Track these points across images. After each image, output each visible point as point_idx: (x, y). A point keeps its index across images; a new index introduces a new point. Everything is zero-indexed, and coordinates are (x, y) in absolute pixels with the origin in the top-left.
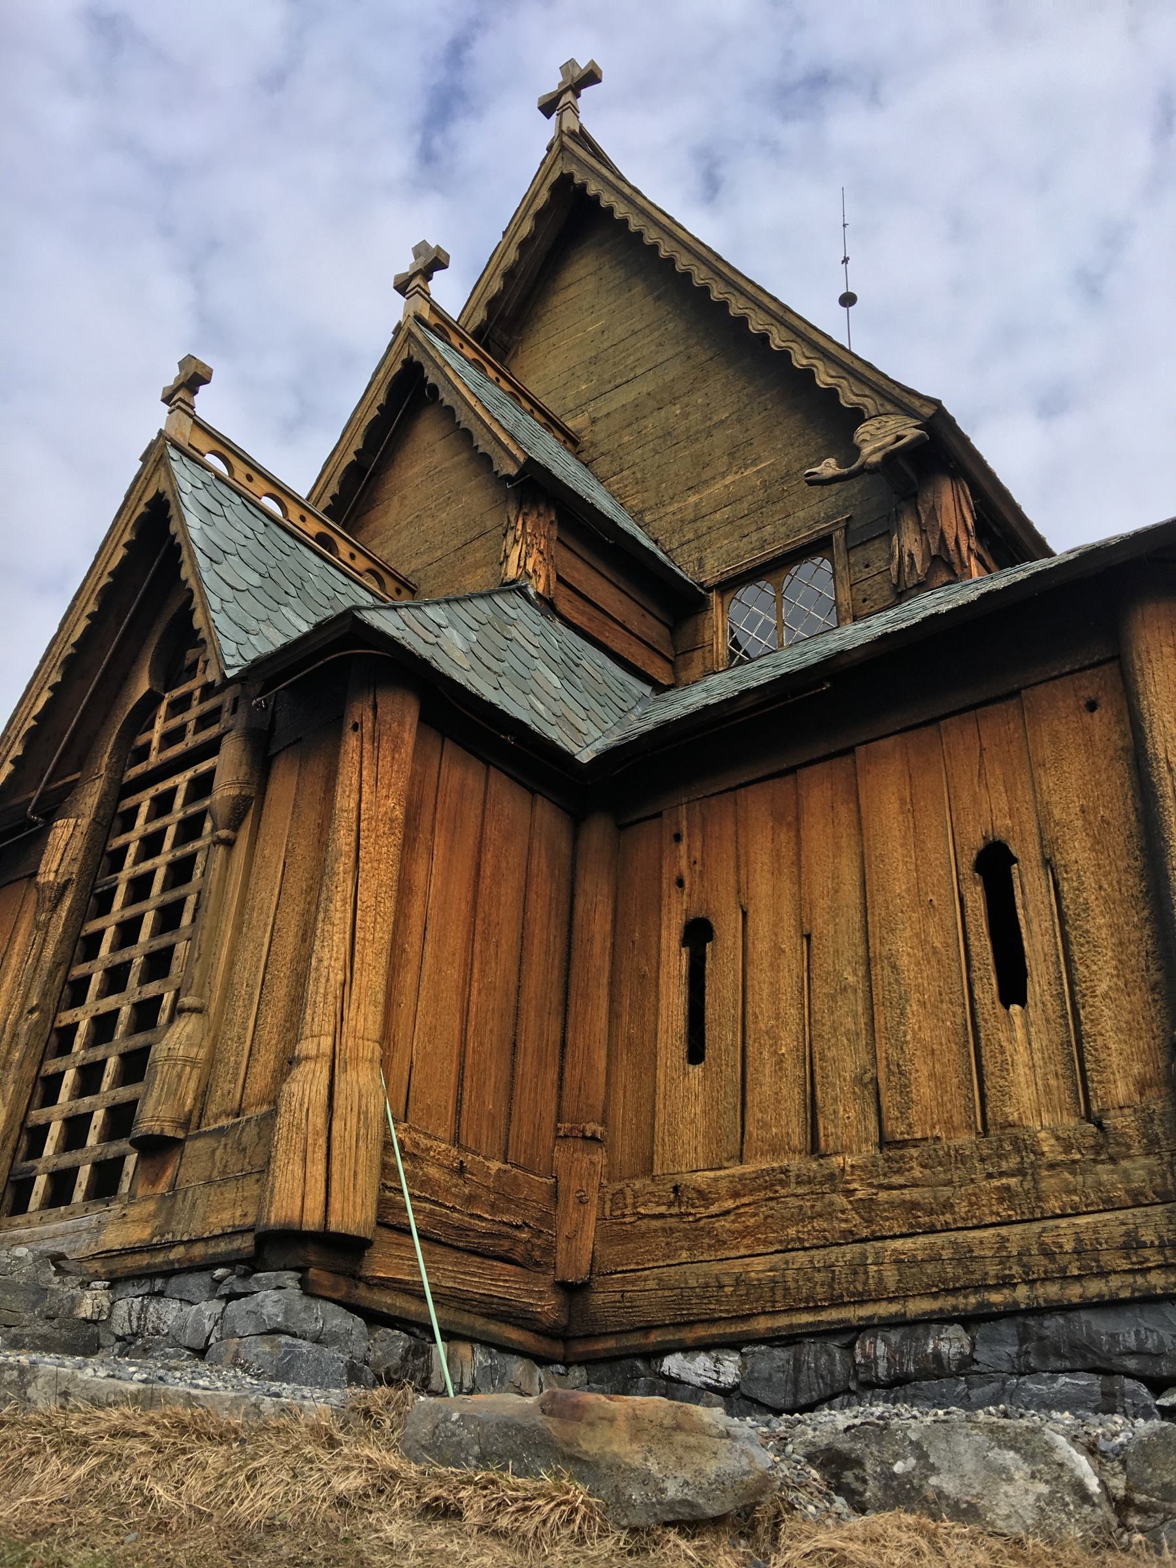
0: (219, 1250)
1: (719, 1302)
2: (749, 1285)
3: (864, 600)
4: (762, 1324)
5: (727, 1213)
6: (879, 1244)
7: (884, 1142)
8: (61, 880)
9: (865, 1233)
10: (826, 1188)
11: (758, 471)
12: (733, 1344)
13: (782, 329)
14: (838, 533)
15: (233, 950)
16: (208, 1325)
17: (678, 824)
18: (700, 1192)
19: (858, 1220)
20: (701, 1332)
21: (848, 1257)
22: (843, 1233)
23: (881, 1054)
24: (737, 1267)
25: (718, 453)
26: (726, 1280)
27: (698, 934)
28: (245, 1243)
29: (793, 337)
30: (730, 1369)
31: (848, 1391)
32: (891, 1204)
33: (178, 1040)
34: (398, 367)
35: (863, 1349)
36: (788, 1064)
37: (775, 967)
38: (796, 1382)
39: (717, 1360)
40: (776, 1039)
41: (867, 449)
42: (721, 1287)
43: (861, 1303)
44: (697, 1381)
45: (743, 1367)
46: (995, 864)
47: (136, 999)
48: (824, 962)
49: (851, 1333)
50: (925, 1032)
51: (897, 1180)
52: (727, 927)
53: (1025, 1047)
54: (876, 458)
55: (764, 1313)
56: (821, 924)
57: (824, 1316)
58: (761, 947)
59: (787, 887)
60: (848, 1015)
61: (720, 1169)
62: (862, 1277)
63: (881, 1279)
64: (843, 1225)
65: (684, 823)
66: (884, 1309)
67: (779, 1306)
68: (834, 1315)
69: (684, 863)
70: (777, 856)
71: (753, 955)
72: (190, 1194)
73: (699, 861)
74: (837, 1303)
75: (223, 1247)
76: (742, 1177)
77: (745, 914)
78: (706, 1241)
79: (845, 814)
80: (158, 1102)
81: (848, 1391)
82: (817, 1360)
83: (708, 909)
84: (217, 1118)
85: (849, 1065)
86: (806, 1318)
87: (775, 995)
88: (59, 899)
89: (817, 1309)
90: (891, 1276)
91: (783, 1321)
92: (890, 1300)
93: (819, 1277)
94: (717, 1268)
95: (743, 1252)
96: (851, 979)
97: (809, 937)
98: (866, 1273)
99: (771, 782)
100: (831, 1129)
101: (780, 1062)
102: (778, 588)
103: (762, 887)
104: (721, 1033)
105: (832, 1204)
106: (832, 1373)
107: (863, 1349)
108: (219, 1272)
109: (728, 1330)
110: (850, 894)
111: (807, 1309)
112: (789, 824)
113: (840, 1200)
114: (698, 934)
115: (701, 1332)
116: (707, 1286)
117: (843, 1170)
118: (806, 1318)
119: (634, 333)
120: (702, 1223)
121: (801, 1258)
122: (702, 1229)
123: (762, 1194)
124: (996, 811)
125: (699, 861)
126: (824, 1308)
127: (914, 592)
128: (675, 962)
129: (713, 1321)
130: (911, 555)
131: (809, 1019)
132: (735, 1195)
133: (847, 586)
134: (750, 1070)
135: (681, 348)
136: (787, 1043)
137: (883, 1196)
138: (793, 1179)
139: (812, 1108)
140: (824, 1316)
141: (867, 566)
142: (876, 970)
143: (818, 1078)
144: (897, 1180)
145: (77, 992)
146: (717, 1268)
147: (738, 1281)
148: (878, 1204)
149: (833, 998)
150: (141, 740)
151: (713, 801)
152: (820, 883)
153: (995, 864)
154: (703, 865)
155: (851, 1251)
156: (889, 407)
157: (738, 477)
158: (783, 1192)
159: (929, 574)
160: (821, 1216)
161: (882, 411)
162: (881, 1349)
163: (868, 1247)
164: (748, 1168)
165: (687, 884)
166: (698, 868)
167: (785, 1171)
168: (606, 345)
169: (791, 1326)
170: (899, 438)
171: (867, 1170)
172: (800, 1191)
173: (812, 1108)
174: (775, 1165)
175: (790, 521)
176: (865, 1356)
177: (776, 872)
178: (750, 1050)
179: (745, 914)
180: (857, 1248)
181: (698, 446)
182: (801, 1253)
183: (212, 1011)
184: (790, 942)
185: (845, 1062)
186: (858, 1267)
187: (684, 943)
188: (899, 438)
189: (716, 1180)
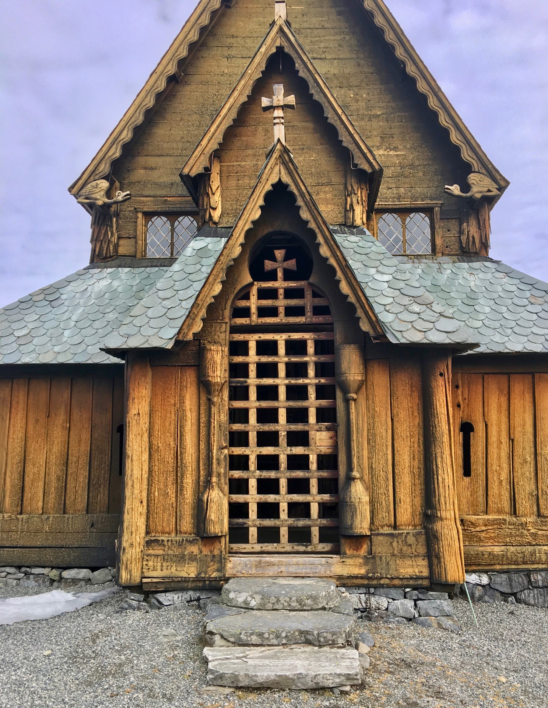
0: (410, 583)
1: (482, 559)
2: (494, 556)
3: (447, 247)
4: (498, 567)
5: (483, 531)
6: (539, 547)
7: (539, 515)
8: (223, 382)
9: (534, 543)
10: (520, 527)
11: (397, 155)
12: (486, 572)
13: (435, 99)
14: (437, 209)
15: (369, 452)
16: (413, 610)
17: (458, 381)
18: (472, 524)
19: (532, 539)
20: (474, 568)
21: (530, 550)
22: (527, 542)
23: (539, 487)
24: (489, 549)
25: (375, 133)
26: (485, 553)
27: (467, 429)
28: (426, 583)
29: (440, 106)
30: (485, 580)
31: (529, 589)
32: (543, 535)
33: (358, 492)
34: (274, 50)
35: (534, 577)
36: (504, 483)
37: (499, 448)
38: (511, 585)
39: (479, 576)
40: (500, 474)
41: (475, 189)
42: (483, 555)
43: (533, 564)
44: (473, 582)
45: (490, 579)
47: (289, 453)
48: (518, 450)
49: (528, 573)
51: (544, 528)
52: (479, 428)
54: (478, 196)
55: (499, 564)
56: (518, 436)
57: (520, 567)
58: (493, 439)
59: (504, 419)
61: (478, 515)
62: (534, 557)
63: (540, 558)
64: (527, 540)
65: (460, 381)
66: (541, 566)
67: (504, 562)
68: (524, 566)
69: (460, 398)
70: (500, 406)
71: (490, 441)
72: (384, 558)
73: (467, 398)
74: (525, 563)
75: (411, 582)
76: (488, 520)
77: (486, 425)
78: (475, 539)
79: (528, 397)
80: (361, 521)
81: (529, 589)
82: (518, 579)
83: (471, 419)
84: (382, 527)
85: (528, 488)
86: (513, 567)
87: (499, 457)
88: (221, 390)
89: (518, 564)
90: (544, 558)
91: (505, 567)
92: (542, 564)
93: (519, 555)
94: (481, 549)
95: (490, 544)
96: (529, 459)
97: (513, 440)
98: (535, 555)
99: (498, 376)
100: (521, 508)
101: (501, 482)
102: (404, 221)
103: (493, 416)
105: (522, 533)
106: (523, 583)
107: (534, 577)
108: (407, 590)
109: (485, 568)
110: (529, 429)
111: (515, 564)
112: (505, 395)
113: (526, 532)
115: (474, 568)
116: (478, 554)
117: (526, 523)
118: (513, 567)
119: (323, 28)
120: (473, 533)
121: (512, 549)
122: (474, 535)
123: (496, 526)
125: (467, 398)
126: (520, 564)
127: (473, 255)
129: (479, 565)
130: (473, 237)
131: (512, 470)
132: (486, 525)
133: (440, 237)
134: (489, 483)
135: (354, 56)
136: (504, 476)
137: (540, 532)
138: (507, 523)
139: (513, 500)
140: (520, 567)
141: (449, 231)
142: (539, 458)
143: (516, 491)
144: (544, 528)
146: (481, 549)
147: (490, 553)
148: (538, 535)
149: (522, 465)
150: (243, 304)
151: (473, 376)
152: (517, 420)
154: (469, 401)
155: (530, 548)
156: (484, 171)
157: (386, 153)
158: (504, 526)
159: (480, 250)
160: (518, 536)
161: (481, 171)
162: (540, 578)
163: (537, 548)
164: (490, 517)
165: (462, 407)
166: (466, 401)
167: (505, 520)
168: (305, 25)
169: (509, 569)
170: (489, 191)
171: (534, 524)
172: (510, 527)
173: (513, 500)
174: (501, 517)
175: (413, 191)
176: (534, 579)
177: (499, 411)
178: (489, 476)
179: (486, 425)
180: (532, 548)
181: (363, 123)
182: (512, 547)
183: (366, 477)
184: (504, 439)
185: (525, 487)
186: (533, 554)
187: (461, 430)
188: (489, 191)
189: (478, 519)
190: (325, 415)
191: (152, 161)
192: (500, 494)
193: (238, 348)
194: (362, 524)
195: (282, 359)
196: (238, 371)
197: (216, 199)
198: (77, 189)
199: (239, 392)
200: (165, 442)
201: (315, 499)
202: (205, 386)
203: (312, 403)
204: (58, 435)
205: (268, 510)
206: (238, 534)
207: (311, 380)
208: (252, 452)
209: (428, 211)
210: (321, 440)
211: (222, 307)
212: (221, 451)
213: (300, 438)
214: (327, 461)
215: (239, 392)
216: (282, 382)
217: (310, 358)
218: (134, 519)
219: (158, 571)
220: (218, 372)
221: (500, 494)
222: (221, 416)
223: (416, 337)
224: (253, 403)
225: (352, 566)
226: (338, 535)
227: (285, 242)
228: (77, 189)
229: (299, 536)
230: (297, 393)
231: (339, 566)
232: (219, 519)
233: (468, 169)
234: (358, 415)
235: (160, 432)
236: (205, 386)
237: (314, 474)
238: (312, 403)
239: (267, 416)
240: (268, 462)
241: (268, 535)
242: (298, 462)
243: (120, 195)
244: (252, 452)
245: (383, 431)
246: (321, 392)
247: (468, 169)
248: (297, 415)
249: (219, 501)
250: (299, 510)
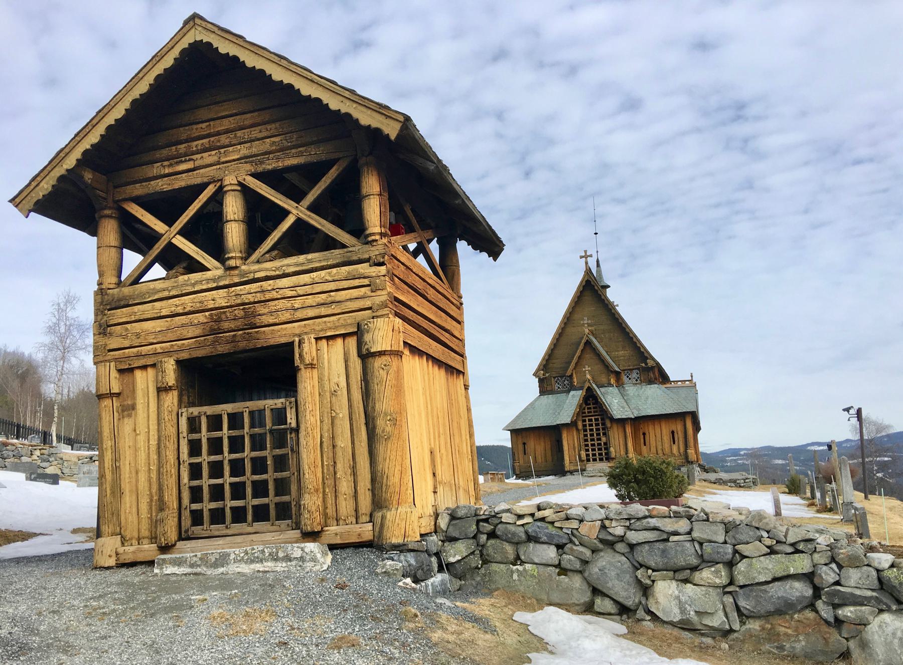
33: (612, 449)
46: (673, 432)
50: (667, 446)
53: (675, 448)
60: (659, 444)
104: (647, 443)
114: (644, 434)
124: (673, 428)
128: (642, 437)
145: (586, 440)
153: (673, 432)
185: (660, 447)
190: (604, 434)
191: (554, 361)
192: (653, 450)
193: (584, 421)
194: (613, 455)
195: (594, 422)
196: (584, 426)
197: (575, 380)
198: (535, 375)
199: (585, 431)
200: (571, 442)
201: (603, 452)
202: (578, 430)
203: (601, 432)
204: (543, 444)
206: (588, 460)
207: (600, 427)
208: (589, 443)
209: (638, 369)
210: (604, 439)
211: (580, 413)
212: (583, 443)
213: (599, 439)
214: (605, 444)
215: (585, 431)
216: (594, 427)
217: (600, 422)
218: (567, 458)
220: (580, 427)
221: (653, 450)
222: (582, 436)
223: (619, 417)
224: (588, 433)
227: (591, 399)
228: (535, 375)
229: (601, 460)
230: (598, 430)
231: (609, 465)
232: (584, 457)
233: (647, 358)
234: (611, 433)
235: (569, 442)
236: (578, 430)
238: (601, 432)
239: (592, 435)
240: (593, 445)
241: (594, 460)
242: (599, 444)
243: (547, 375)
244: (589, 443)
245: (616, 436)
246: (603, 429)
247: (647, 358)
248: (598, 434)
249: (583, 454)
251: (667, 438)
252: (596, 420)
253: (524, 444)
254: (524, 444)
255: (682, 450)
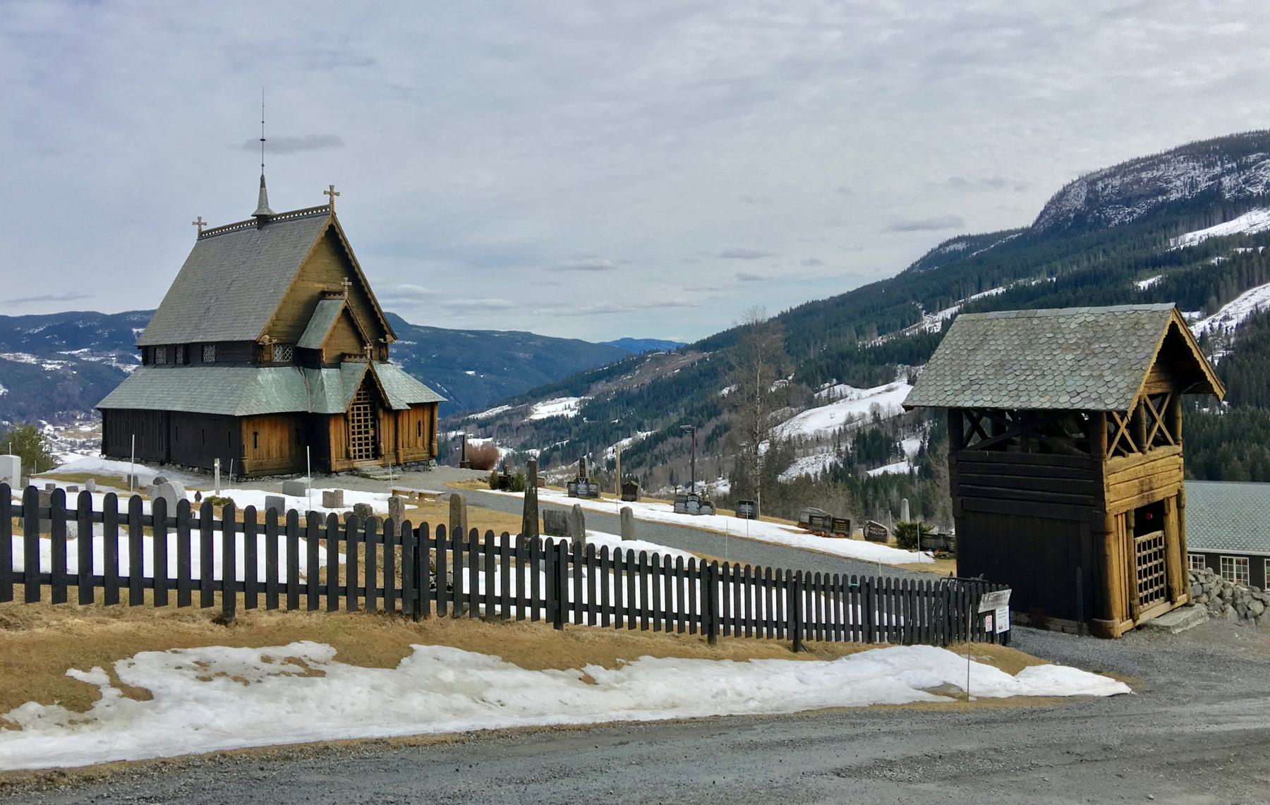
201: (370, 447)
202: (346, 420)
203: (370, 423)
204: (279, 433)
205: (360, 451)
213: (367, 432)
219: (339, 468)
225: (380, 462)
226: (376, 454)
229: (367, 456)
230: (366, 421)
236: (346, 420)
237: (370, 441)
241: (361, 457)
248: (366, 426)
250: (367, 450)
251: (413, 429)
252: (365, 409)
253: (256, 434)
254: (256, 434)
255: (426, 442)
